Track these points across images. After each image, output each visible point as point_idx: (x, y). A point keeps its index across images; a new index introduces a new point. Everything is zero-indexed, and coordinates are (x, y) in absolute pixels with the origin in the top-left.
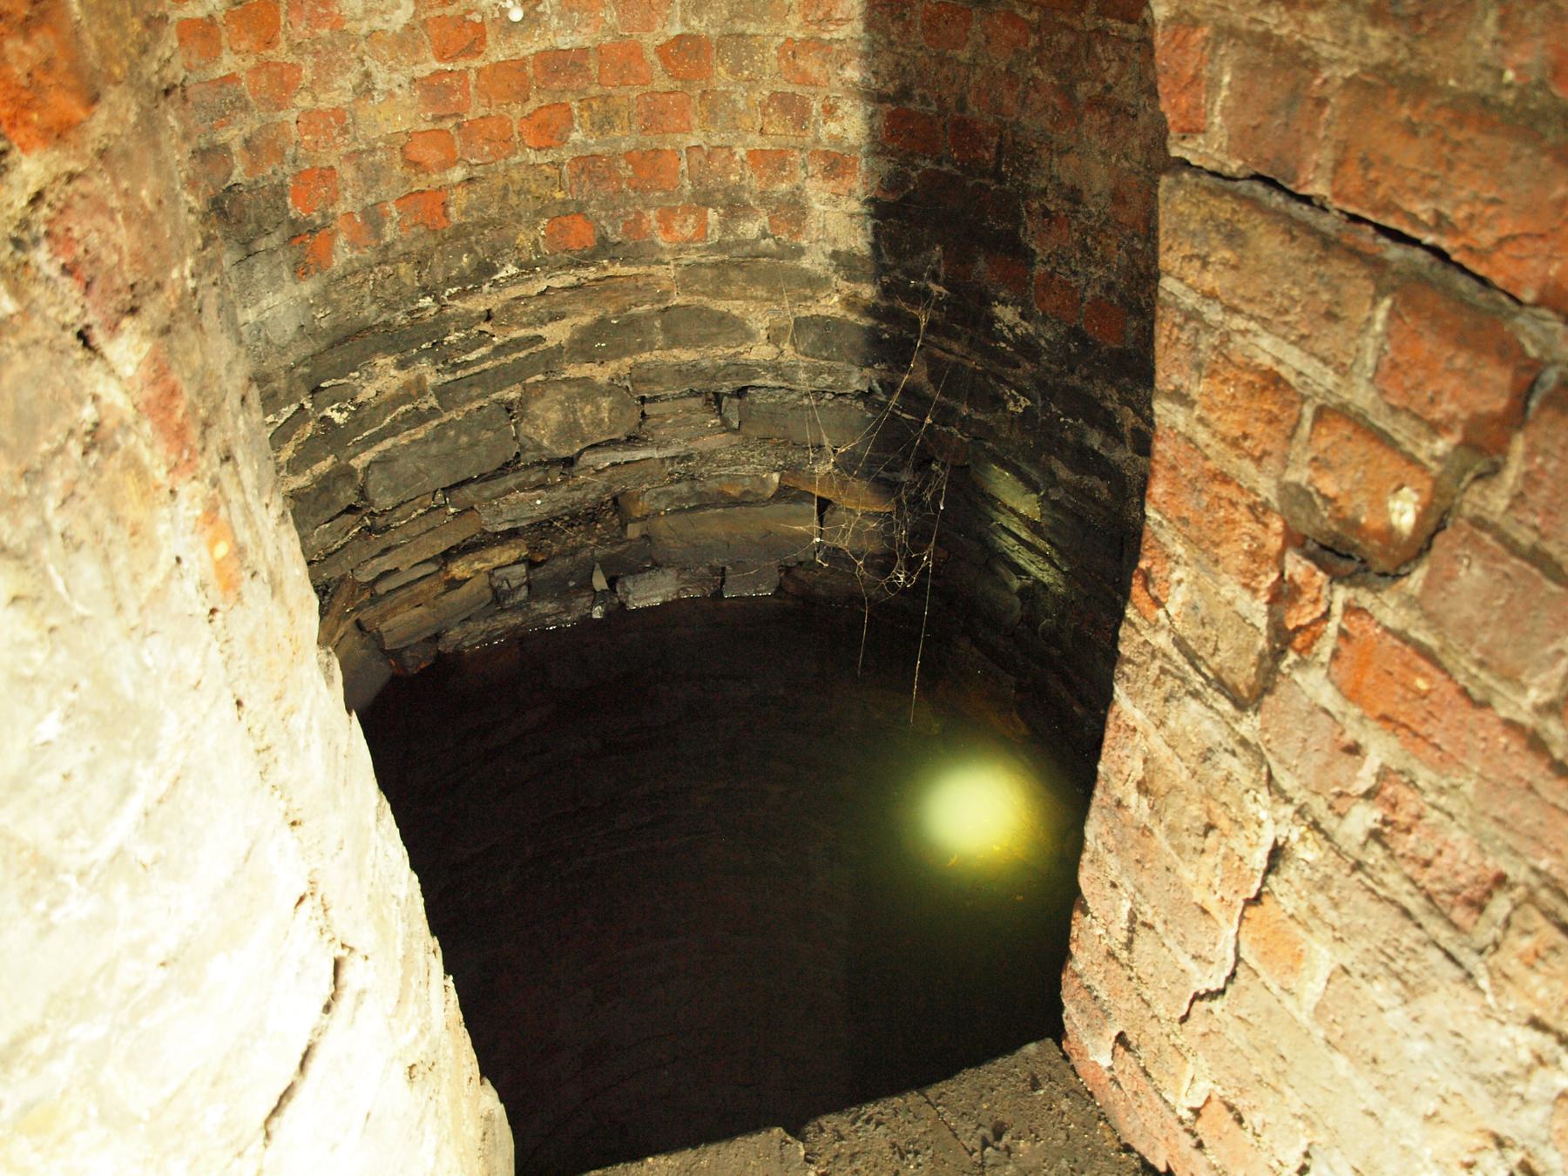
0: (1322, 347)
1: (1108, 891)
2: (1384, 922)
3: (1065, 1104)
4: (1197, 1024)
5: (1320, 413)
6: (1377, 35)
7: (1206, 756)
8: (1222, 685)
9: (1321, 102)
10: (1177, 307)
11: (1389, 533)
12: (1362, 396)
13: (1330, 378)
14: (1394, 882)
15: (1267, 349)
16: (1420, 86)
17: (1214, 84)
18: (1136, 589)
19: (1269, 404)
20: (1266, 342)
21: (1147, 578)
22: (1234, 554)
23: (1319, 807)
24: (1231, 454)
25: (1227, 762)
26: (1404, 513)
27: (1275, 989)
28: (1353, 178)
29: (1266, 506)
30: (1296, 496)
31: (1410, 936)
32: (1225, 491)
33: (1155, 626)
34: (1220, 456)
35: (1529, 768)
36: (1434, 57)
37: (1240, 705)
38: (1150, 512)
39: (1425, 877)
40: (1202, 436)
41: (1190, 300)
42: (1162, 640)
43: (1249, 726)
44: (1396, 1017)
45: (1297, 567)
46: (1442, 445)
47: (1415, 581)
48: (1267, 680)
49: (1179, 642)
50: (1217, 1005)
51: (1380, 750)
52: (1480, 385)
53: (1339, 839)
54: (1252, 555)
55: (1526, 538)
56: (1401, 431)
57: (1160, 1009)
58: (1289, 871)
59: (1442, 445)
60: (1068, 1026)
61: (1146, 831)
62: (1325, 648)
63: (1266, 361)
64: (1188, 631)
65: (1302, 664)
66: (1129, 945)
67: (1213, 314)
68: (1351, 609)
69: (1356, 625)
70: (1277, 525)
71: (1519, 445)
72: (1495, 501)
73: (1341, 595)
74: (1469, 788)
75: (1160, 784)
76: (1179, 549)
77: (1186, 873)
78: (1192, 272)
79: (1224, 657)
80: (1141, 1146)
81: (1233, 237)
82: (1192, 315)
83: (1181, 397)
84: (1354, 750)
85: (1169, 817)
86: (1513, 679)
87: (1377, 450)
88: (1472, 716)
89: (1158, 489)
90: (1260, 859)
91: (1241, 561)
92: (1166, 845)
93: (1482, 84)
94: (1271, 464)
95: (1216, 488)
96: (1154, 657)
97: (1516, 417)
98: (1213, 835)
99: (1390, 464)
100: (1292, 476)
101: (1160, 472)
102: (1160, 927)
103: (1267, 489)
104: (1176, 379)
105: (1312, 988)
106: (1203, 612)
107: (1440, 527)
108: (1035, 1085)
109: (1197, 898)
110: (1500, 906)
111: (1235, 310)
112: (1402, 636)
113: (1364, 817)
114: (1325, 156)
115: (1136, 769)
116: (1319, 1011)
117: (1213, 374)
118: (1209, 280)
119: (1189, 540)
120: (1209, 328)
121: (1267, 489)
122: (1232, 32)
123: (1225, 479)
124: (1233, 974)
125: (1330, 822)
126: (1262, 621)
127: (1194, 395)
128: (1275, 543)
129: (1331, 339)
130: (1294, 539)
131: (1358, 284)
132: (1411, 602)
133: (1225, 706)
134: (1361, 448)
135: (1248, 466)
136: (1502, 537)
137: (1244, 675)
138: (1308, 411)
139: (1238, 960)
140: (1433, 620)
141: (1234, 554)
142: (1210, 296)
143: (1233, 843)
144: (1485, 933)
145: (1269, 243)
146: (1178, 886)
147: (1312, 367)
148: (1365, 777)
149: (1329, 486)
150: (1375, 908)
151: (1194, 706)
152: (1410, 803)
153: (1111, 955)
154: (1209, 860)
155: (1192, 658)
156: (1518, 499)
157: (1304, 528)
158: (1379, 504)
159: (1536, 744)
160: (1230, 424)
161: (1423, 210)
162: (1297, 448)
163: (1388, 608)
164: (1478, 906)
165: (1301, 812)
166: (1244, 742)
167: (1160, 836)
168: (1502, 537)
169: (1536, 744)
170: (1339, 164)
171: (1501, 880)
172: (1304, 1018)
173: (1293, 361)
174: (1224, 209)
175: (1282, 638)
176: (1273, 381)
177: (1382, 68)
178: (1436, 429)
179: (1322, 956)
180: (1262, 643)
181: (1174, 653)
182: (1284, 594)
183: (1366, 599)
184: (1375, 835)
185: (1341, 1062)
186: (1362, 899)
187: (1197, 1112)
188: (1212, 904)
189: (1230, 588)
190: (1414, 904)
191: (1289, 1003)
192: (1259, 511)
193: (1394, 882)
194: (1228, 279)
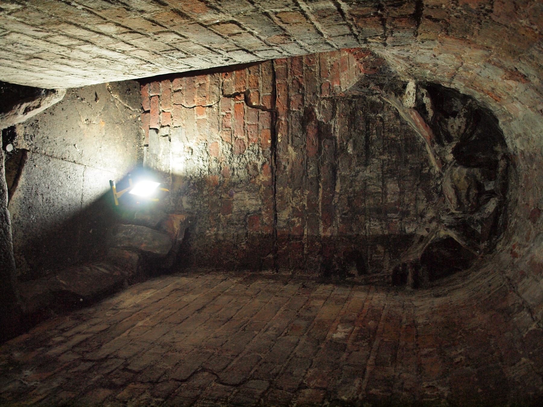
0: (264, 89)
1: (179, 85)
2: (216, 121)
3: (138, 93)
4: (178, 106)
5: (258, 91)
6: (291, 83)
7: (213, 92)
8: (222, 90)
9: (284, 80)
10: (259, 68)
11: (252, 103)
12: (261, 95)
13: (261, 91)
14: (221, 120)
15: (260, 82)
16: (288, 90)
17: (282, 65)
18: (224, 74)
19: (255, 85)
20: (261, 82)
21: (226, 75)
22: (238, 86)
23: (220, 109)
24: (248, 82)
25: (215, 96)
26: (254, 104)
27: (195, 114)
28: (279, 86)
29: (245, 89)
30: (248, 92)
31: (217, 124)
32: (244, 82)
33: (222, 79)
34: (247, 80)
35: (242, 125)
36: (291, 90)
37: (223, 94)
38: (234, 72)
39: (224, 122)
40: (248, 77)
41: (260, 70)
42: (221, 80)
43: (221, 96)
44: (208, 127)
45: (243, 95)
46: (262, 105)
47: (250, 108)
48: (229, 96)
49: (223, 83)
50: (183, 108)
51: (232, 112)
52: (268, 106)
53: (219, 112)
54: (239, 88)
55: (259, 116)
56: (261, 100)
57: (173, 101)
58: (211, 109)
59: (262, 105)
60: (147, 85)
61: (195, 87)
62: (237, 102)
63: (259, 82)
64: (225, 83)
65: (234, 100)
66: (175, 92)
67: (261, 74)
68: (243, 103)
69: (242, 104)
70: (245, 91)
71: (266, 112)
72: (261, 112)
73: (243, 101)
74: (236, 121)
75: (203, 87)
76: (233, 78)
77: (196, 96)
78: (263, 69)
79: (226, 90)
80: (143, 105)
81: (269, 73)
82: (259, 70)
83: (250, 72)
84: (230, 110)
85: (200, 91)
86: (248, 120)
87: (258, 98)
88: (242, 119)
89: (238, 72)
90: (208, 105)
91: (238, 88)
92: (196, 92)
93: (290, 95)
94: (250, 87)
95: (243, 81)
96: (218, 80)
97: (267, 110)
98: (204, 98)
99: (258, 101)
100: (250, 90)
101: (240, 72)
102: (184, 95)
103: (247, 88)
104: (251, 70)
105: (201, 117)
106: (229, 84)
107: (255, 108)
108: (135, 88)
109: (194, 99)
110: (228, 129)
111: (262, 76)
112: (244, 109)
113: (224, 114)
114: (280, 82)
115: (202, 83)
116: (198, 120)
117: (255, 76)
118: (263, 71)
119: (235, 79)
120: (259, 73)
121: (247, 88)
122: (287, 66)
123: (245, 82)
124: (191, 108)
125: (220, 110)
126: (233, 93)
127: (251, 74)
128: (242, 91)
129: (265, 89)
130: (244, 93)
131: (271, 90)
132: (248, 108)
133: (221, 93)
134: (258, 97)
135: (248, 85)
136: (258, 113)
137: (226, 93)
138: (257, 90)
139: (193, 107)
140: (247, 111)
141: (238, 86)
142: (262, 72)
143: (207, 101)
144: (225, 129)
145: (270, 78)
146: (193, 96)
147: (261, 88)
148: (228, 112)
149: (252, 95)
150: (216, 119)
151: (218, 88)
152: (230, 117)
153: (170, 89)
154: (201, 99)
155: (222, 85)
156: (262, 113)
157: (246, 94)
158: (254, 101)
159: (244, 125)
160: (251, 80)
161: (279, 94)
162: (253, 90)
163: (246, 107)
164: (226, 128)
165: (218, 107)
166: (219, 97)
167: (197, 90)
168: (258, 113)
169: (244, 125)
170: (279, 83)
171: (230, 128)
172: (196, 118)
173: (260, 86)
174: (271, 71)
175: (234, 96)
176: (258, 84)
177: (288, 85)
178: (263, 103)
179: (205, 116)
180: (231, 94)
181: (221, 83)
182: (238, 94)
183: (245, 104)
184: (223, 115)
185: (196, 124)
186: (216, 118)
187: (163, 111)
188: (196, 101)
189: (234, 88)
190: (220, 122)
191: (196, 116)
192: (244, 88)
193: (221, 120)
194: (265, 74)
